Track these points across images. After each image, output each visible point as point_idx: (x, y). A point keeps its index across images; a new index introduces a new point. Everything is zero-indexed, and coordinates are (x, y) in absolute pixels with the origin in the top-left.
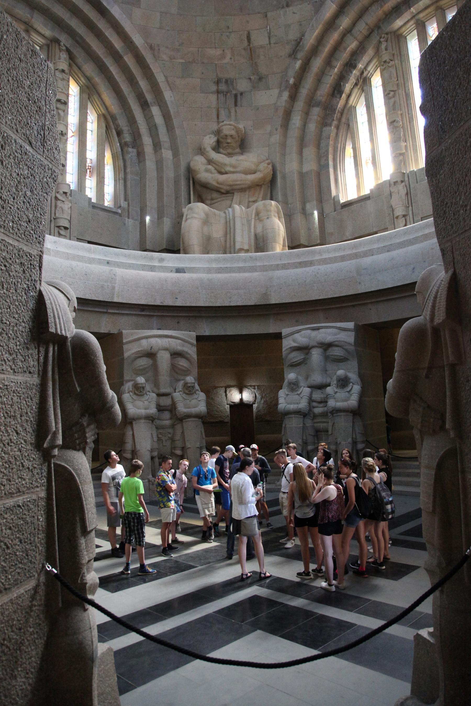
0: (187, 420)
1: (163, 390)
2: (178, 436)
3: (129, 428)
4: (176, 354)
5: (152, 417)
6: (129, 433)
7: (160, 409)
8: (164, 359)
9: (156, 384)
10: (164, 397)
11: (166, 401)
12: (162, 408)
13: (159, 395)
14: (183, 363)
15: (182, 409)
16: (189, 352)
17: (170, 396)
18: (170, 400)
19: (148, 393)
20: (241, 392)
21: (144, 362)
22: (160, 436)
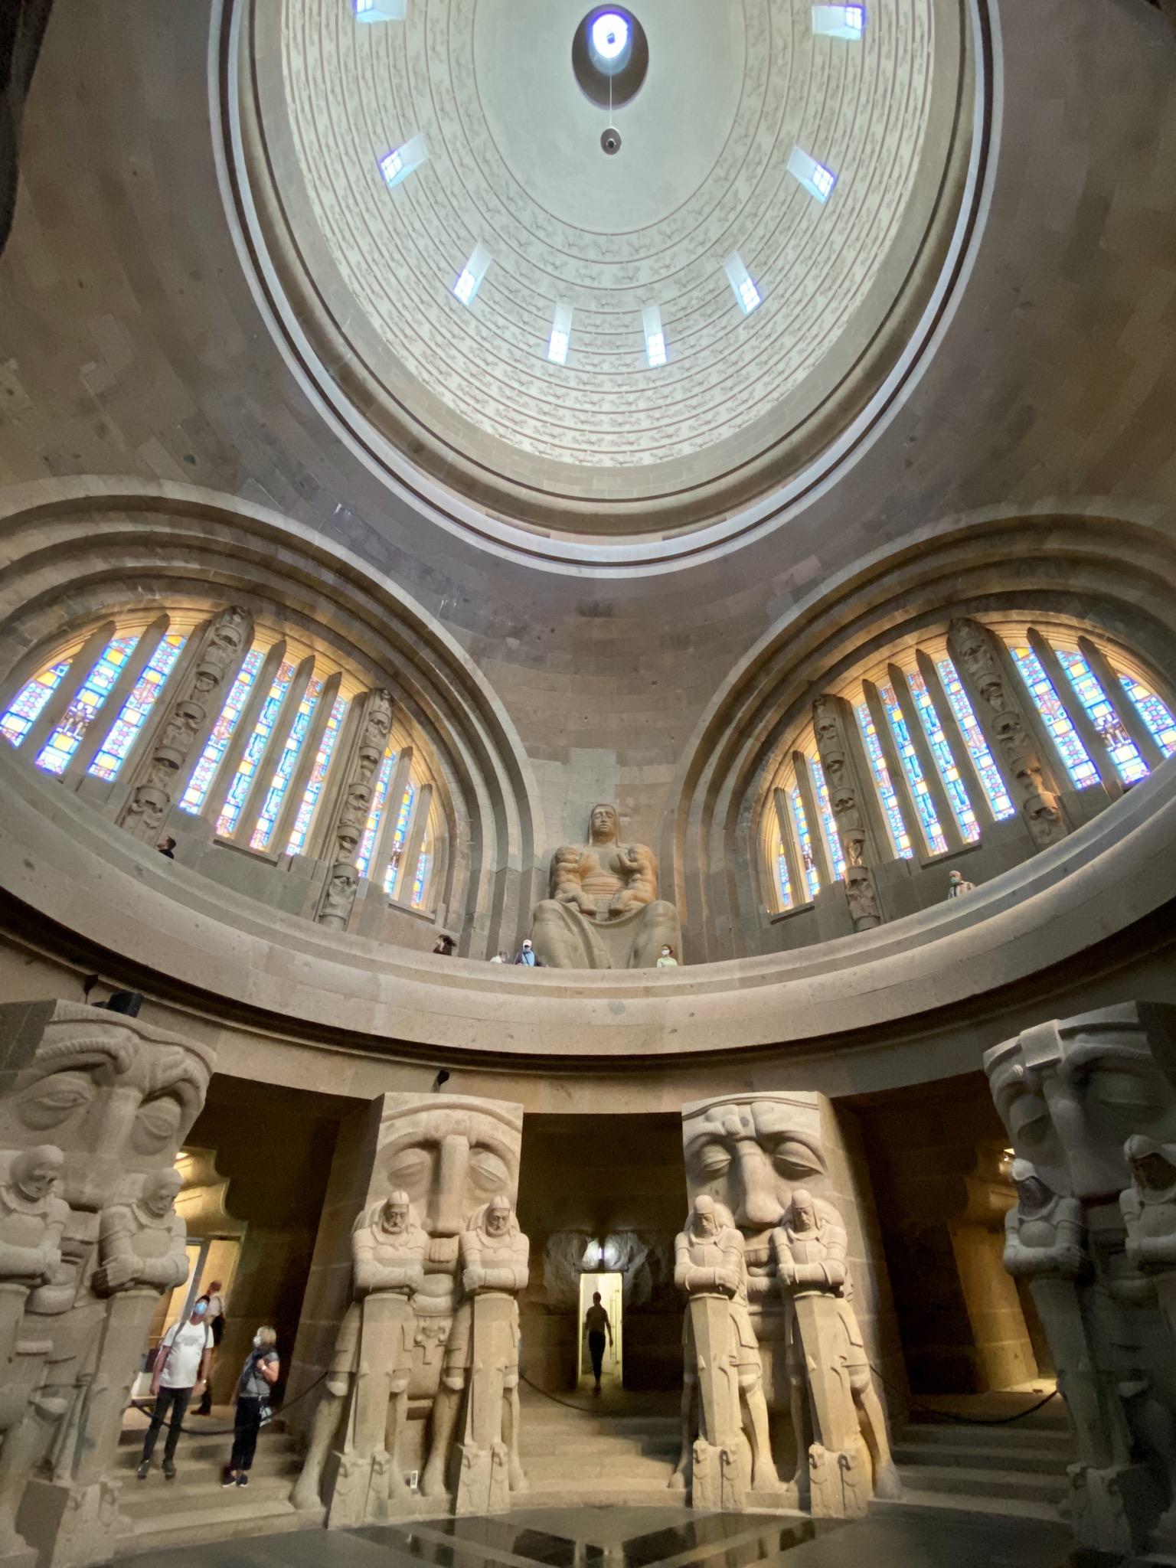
0: (483, 1296)
1: (443, 1225)
2: (462, 1342)
3: (354, 1313)
4: (481, 1146)
5: (408, 1286)
6: (354, 1325)
7: (433, 1268)
8: (458, 1149)
9: (433, 1209)
10: (444, 1240)
11: (447, 1250)
12: (436, 1266)
13: (434, 1234)
14: (490, 1163)
15: (476, 1272)
16: (507, 1141)
17: (457, 1238)
18: (456, 1247)
19: (411, 1229)
20: (602, 1245)
21: (420, 1158)
22: (420, 1338)
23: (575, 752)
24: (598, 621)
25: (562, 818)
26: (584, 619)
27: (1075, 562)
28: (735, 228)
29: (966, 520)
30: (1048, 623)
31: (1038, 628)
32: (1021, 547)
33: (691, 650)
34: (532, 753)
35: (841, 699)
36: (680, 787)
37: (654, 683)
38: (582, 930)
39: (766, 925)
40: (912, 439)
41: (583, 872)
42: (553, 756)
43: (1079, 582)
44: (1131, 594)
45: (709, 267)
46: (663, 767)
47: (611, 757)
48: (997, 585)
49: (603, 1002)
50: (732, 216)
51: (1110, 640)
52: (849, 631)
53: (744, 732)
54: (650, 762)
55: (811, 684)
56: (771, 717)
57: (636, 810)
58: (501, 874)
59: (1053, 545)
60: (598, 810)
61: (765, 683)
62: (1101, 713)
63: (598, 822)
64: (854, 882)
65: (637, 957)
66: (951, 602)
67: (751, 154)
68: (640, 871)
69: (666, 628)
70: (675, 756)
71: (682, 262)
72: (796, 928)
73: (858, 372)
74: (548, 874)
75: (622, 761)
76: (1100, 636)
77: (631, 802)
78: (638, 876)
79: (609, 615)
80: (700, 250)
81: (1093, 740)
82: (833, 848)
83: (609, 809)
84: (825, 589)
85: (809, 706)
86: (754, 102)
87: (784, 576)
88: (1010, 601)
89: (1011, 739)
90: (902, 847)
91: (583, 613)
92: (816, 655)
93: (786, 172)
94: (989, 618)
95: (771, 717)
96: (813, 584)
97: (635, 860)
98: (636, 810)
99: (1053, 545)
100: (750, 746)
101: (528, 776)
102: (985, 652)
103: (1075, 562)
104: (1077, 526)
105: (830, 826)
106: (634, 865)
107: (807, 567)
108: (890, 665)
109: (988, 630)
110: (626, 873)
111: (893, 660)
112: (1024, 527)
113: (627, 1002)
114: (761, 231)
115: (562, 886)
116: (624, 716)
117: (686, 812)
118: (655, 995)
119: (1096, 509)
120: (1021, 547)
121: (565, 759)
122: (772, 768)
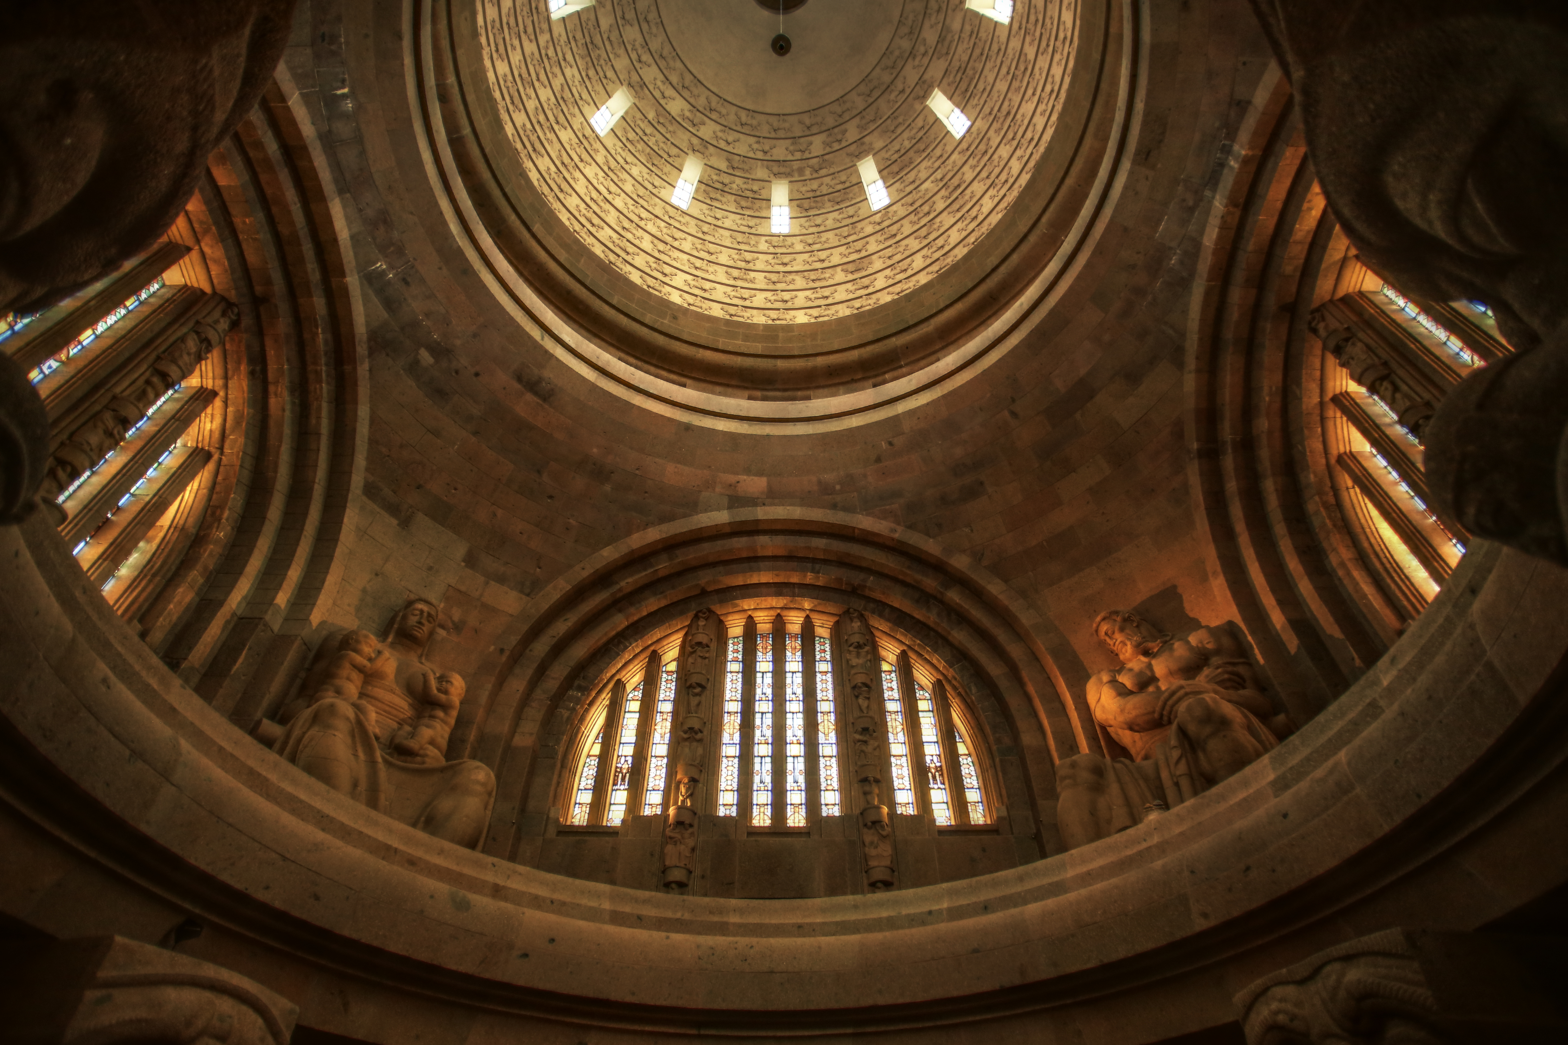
23: (420, 517)
24: (529, 397)
25: (364, 591)
26: (517, 386)
27: (961, 619)
28: (796, 165)
29: (900, 533)
30: (920, 655)
31: (911, 655)
32: (930, 583)
33: (608, 488)
34: (370, 490)
35: (721, 622)
36: (525, 628)
37: (551, 497)
38: (372, 762)
39: (551, 832)
40: (891, 444)
41: (370, 677)
42: (393, 510)
43: (959, 636)
44: (995, 669)
45: (761, 173)
46: (514, 594)
47: (460, 550)
48: (898, 600)
49: (442, 888)
50: (798, 155)
51: (959, 694)
52: (762, 564)
53: (617, 604)
54: (501, 579)
55: (704, 593)
56: (652, 604)
57: (458, 628)
58: (244, 625)
59: (954, 596)
60: (420, 606)
61: (663, 566)
62: (932, 752)
63: (413, 620)
64: (679, 823)
65: (430, 822)
66: (854, 592)
67: (836, 130)
68: (445, 707)
69: (595, 450)
70: (530, 587)
71: (741, 149)
72: (588, 852)
73: (854, 355)
74: (311, 655)
75: (470, 561)
76: (955, 688)
77: (456, 614)
78: (440, 714)
79: (545, 400)
80: (760, 155)
81: (921, 774)
82: (656, 775)
83: (433, 613)
84: (763, 513)
85: (691, 614)
86: (860, 104)
87: (731, 478)
88: (901, 620)
89: (865, 742)
90: (726, 802)
91: (519, 379)
92: (721, 568)
93: (855, 165)
94: (879, 624)
95: (652, 604)
96: (753, 502)
97: (446, 692)
98: (458, 628)
99: (954, 596)
100: (619, 622)
101: (351, 518)
102: (867, 652)
103: (961, 619)
104: (976, 593)
105: (660, 746)
106: (443, 697)
107: (755, 485)
108: (779, 615)
109: (872, 633)
110: (425, 703)
111: (784, 613)
112: (938, 567)
113: (476, 899)
114: (815, 185)
115: (338, 682)
116: (500, 512)
117: (517, 657)
118: (506, 899)
119: (995, 588)
120: (930, 583)
121: (405, 523)
122: (627, 656)
